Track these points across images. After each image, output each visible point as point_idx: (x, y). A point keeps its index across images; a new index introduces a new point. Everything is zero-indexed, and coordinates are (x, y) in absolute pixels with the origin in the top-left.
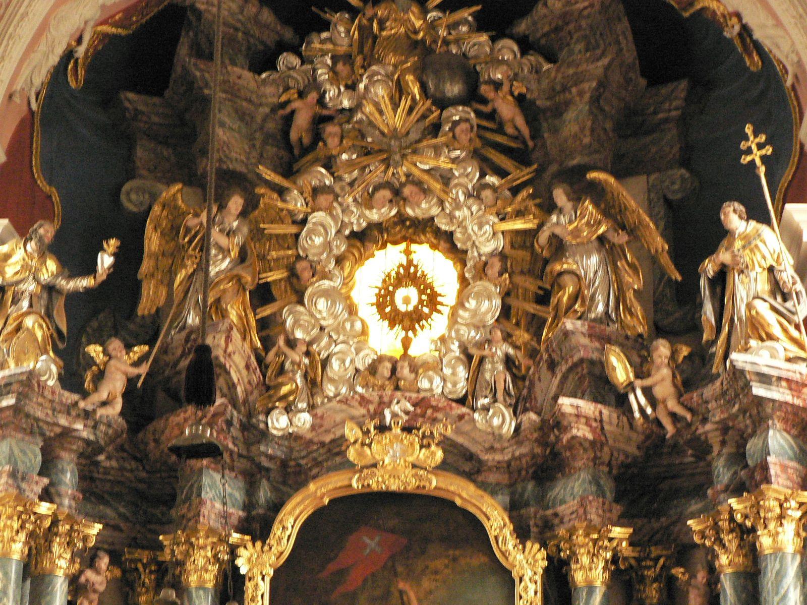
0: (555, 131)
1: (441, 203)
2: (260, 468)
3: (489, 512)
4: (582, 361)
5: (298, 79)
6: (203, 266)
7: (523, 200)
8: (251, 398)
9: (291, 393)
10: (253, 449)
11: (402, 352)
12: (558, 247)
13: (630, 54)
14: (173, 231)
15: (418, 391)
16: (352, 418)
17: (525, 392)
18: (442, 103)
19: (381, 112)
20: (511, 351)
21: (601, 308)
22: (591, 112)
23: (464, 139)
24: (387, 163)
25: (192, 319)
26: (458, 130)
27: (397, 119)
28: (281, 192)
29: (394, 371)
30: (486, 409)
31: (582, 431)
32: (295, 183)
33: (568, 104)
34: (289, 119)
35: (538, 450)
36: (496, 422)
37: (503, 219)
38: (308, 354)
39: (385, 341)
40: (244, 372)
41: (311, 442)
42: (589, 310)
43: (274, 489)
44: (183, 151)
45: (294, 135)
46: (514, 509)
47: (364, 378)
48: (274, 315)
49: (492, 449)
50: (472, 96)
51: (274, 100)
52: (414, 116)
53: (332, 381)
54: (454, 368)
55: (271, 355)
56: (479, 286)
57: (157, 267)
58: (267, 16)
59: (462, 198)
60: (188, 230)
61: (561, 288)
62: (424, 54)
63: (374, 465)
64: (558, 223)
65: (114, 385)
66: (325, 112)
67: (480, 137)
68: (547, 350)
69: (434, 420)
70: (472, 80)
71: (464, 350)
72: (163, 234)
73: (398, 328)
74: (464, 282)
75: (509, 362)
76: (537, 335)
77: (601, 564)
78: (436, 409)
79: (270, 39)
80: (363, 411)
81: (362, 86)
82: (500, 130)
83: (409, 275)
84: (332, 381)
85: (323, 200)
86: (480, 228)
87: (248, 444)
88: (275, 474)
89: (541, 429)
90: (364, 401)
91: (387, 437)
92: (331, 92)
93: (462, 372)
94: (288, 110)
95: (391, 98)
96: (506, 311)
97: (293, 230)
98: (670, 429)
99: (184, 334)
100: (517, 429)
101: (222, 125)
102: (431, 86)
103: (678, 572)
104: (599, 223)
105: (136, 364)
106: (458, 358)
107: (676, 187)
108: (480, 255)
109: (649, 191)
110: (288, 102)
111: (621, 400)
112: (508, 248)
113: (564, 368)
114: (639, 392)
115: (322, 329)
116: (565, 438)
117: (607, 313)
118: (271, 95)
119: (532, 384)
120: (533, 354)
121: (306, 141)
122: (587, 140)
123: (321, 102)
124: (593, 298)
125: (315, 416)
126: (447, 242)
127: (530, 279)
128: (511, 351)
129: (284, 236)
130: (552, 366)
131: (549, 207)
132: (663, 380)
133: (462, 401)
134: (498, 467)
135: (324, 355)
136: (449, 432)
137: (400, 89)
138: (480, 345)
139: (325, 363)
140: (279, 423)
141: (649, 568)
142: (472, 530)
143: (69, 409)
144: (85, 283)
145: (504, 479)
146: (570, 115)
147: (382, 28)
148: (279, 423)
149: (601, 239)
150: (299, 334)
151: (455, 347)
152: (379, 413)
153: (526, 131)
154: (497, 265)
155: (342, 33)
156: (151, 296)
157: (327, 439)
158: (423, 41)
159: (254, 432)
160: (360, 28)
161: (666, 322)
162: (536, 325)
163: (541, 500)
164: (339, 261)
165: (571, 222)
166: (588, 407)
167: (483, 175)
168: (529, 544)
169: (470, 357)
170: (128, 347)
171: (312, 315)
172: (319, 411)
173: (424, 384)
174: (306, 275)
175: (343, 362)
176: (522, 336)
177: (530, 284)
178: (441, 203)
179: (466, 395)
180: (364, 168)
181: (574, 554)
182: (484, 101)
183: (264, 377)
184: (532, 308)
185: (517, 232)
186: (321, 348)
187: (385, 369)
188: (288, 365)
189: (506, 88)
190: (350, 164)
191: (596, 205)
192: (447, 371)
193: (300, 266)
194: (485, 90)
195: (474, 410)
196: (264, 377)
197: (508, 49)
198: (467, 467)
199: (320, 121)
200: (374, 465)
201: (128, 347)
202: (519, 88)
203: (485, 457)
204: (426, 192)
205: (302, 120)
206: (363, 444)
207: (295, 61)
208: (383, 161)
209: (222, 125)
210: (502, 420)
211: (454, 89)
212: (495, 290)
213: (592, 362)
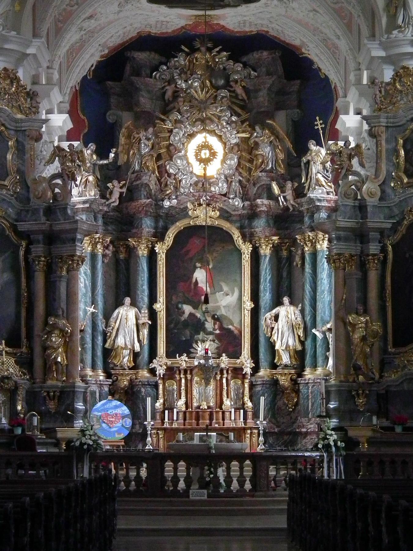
0: (256, 98)
1: (217, 126)
2: (159, 216)
3: (234, 232)
4: (264, 184)
5: (168, 77)
6: (139, 150)
7: (245, 127)
8: (157, 194)
9: (170, 193)
10: (158, 211)
11: (203, 172)
14: (129, 137)
15: (211, 192)
16: (190, 201)
17: (245, 192)
18: (217, 88)
19: (196, 92)
20: (241, 179)
21: (270, 166)
22: (268, 94)
23: (225, 104)
24: (199, 110)
25: (137, 168)
26: (223, 100)
28: (163, 121)
29: (203, 185)
30: (233, 199)
31: (264, 208)
32: (168, 117)
33: (260, 90)
34: (164, 93)
35: (250, 212)
36: (236, 203)
37: (238, 133)
38: (175, 179)
39: (198, 169)
40: (154, 186)
41: (176, 208)
42: (267, 166)
43: (164, 222)
45: (166, 97)
46: (241, 228)
47: (193, 187)
48: (162, 164)
49: (234, 210)
50: (227, 85)
51: (160, 87)
52: (208, 95)
53: (183, 187)
54: (222, 184)
55: (163, 180)
56: (230, 156)
57: (124, 149)
58: (157, 57)
59: (225, 124)
60: (134, 138)
61: (258, 160)
62: (211, 71)
63: (197, 217)
64: (256, 137)
66: (177, 89)
67: (230, 101)
68: (253, 180)
69: (216, 202)
71: (226, 177)
72: (126, 138)
73: (202, 164)
74: (225, 154)
75: (240, 182)
76: (250, 173)
77: (269, 248)
78: (217, 198)
79: (157, 63)
80: (193, 199)
81: (190, 82)
82: (236, 97)
83: (205, 146)
84: (183, 187)
85: (178, 125)
86: (231, 136)
87: (156, 209)
89: (251, 206)
90: (194, 196)
91: (201, 208)
92: (179, 82)
93: (225, 185)
94: (165, 90)
95: (200, 87)
96: (239, 164)
97: (168, 135)
98: (291, 209)
99: (136, 174)
100: (243, 205)
101: (143, 96)
102: (213, 81)
103: (293, 249)
104: (270, 137)
105: (121, 188)
106: (224, 180)
107: (296, 116)
108: (231, 144)
109: (287, 116)
110: (165, 86)
111: (276, 199)
112: (240, 142)
113: (258, 185)
114: (282, 197)
115: (179, 169)
116: (258, 210)
117: (272, 167)
118: (159, 85)
119: (248, 191)
120: (248, 181)
121: (171, 99)
122: (266, 104)
123: (176, 87)
124: (268, 162)
125: (178, 200)
126: (220, 137)
127: (247, 151)
128: (241, 179)
129: (165, 137)
130: (254, 184)
131: (254, 129)
133: (225, 195)
134: (236, 215)
135: (180, 178)
136: (221, 206)
137: (203, 86)
138: (231, 176)
139: (180, 181)
140: (167, 204)
141: (283, 246)
142: (229, 238)
143: (102, 204)
144: (105, 162)
145: (238, 218)
146: (261, 94)
147: (197, 61)
148: (167, 204)
149: (271, 142)
150: (171, 171)
151: (223, 177)
152: (199, 200)
153: (246, 98)
154: (236, 148)
155: (181, 60)
157: (182, 207)
158: (211, 65)
160: (189, 61)
161: (292, 163)
162: (250, 170)
163: (250, 226)
164: (183, 144)
165: (261, 137)
166: (266, 202)
167: (232, 115)
168: (246, 243)
169: (228, 181)
170: (119, 183)
171: (176, 165)
172: (179, 198)
173: (213, 189)
174: (174, 151)
175: (186, 181)
176: (245, 174)
177: (248, 157)
178: (217, 126)
179: (226, 193)
180: (191, 113)
181: (260, 245)
182: (232, 87)
183: (161, 186)
184: (248, 165)
185: (243, 137)
186: (180, 176)
187: (200, 185)
188: (168, 183)
189: (239, 84)
190: (187, 111)
191: (269, 130)
192: (220, 185)
193: (171, 148)
194: (231, 83)
195: (229, 198)
196: (161, 186)
197: (239, 67)
198: (226, 215)
199: (176, 94)
200: (197, 217)
201: (119, 183)
202: (243, 84)
203: (232, 213)
204: (212, 121)
205: (169, 94)
206: (194, 210)
207: (165, 68)
208: (198, 110)
209: (143, 96)
210: (238, 203)
211: (221, 82)
212: (236, 157)
213: (267, 184)
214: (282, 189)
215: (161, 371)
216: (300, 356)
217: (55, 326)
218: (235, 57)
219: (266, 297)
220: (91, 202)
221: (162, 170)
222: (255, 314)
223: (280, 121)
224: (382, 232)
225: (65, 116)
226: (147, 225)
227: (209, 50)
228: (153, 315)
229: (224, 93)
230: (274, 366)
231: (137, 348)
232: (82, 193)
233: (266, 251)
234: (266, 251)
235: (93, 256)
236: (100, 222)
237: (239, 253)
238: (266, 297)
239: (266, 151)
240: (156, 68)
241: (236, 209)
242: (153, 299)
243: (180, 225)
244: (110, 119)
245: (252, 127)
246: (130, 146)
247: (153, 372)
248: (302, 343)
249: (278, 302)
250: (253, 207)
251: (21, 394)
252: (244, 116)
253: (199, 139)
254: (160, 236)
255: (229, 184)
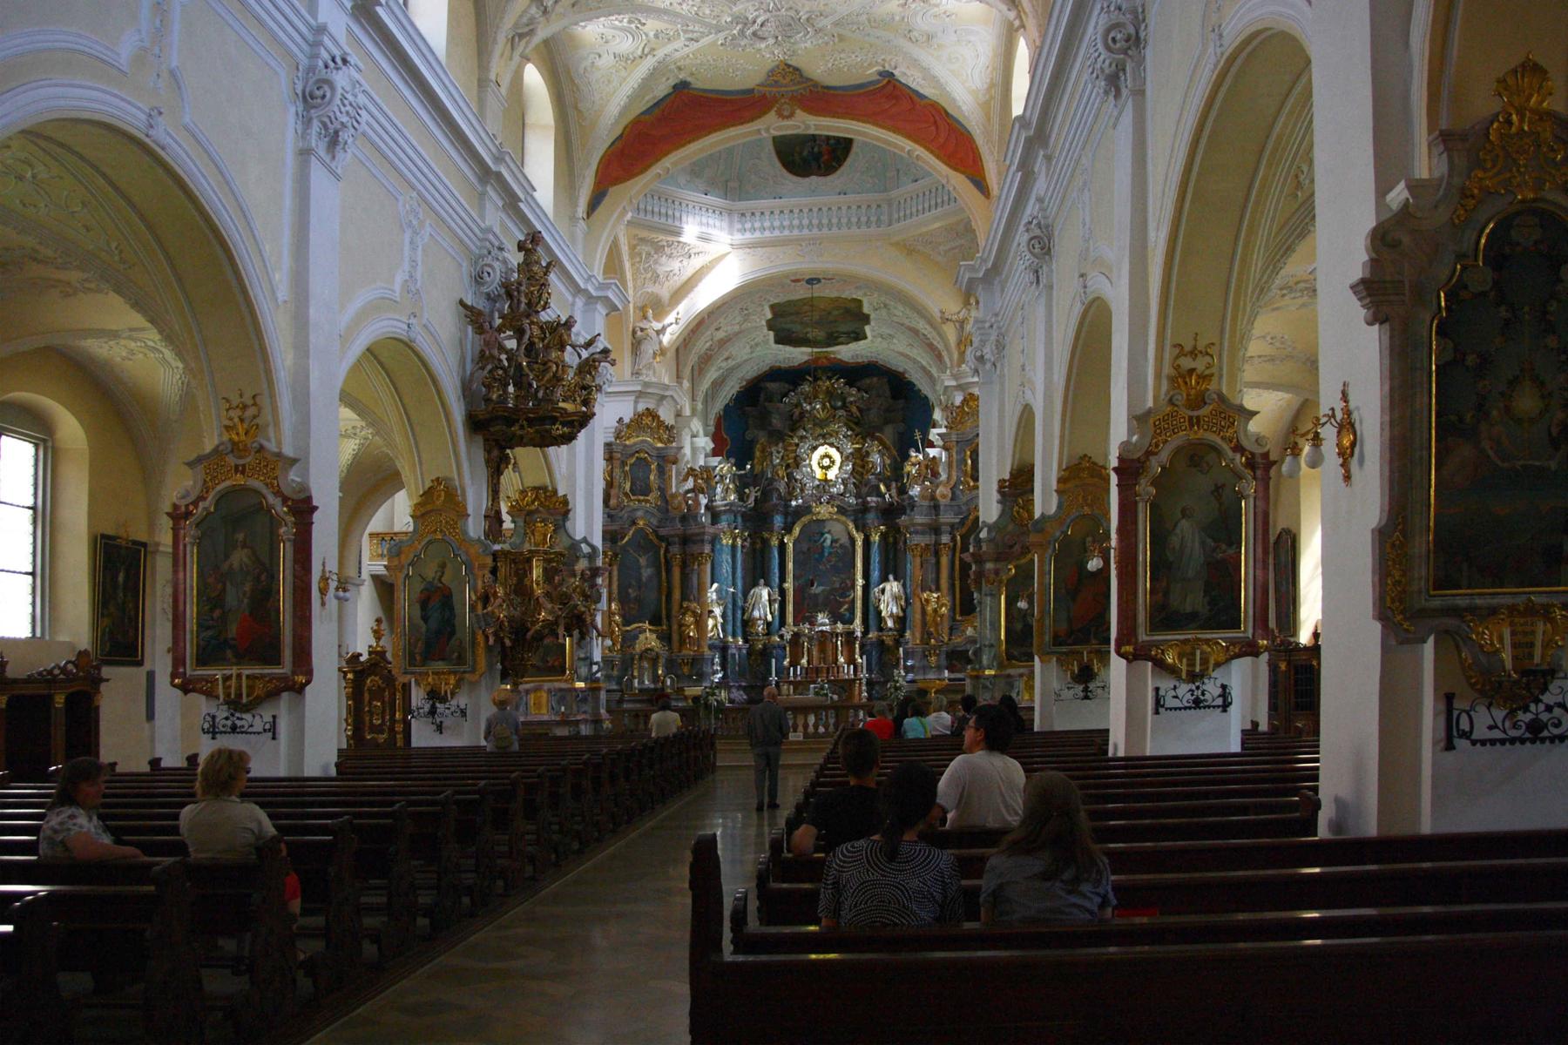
12: (868, 454)
13: (888, 393)
14: (763, 451)
18: (835, 408)
27: (822, 415)
44: (763, 421)
50: (844, 407)
62: (830, 394)
65: (752, 500)
70: (844, 400)
83: (827, 456)
88: (793, 516)
111: (882, 496)
127: (859, 460)
132: (894, 492)
155: (806, 388)
156: (758, 469)
159: (787, 506)
210: (852, 500)
214: (888, 488)
215: (788, 637)
216: (901, 621)
217: (688, 609)
218: (850, 384)
219: (875, 574)
220: (731, 504)
221: (790, 476)
222: (866, 589)
223: (888, 434)
224: (952, 526)
225: (708, 439)
226: (778, 520)
227: (830, 378)
228: (782, 592)
229: (841, 412)
230: (881, 629)
231: (769, 618)
232: (724, 495)
233: (876, 538)
234: (876, 538)
235: (734, 547)
236: (739, 519)
237: (853, 541)
238: (875, 574)
239: (876, 458)
240: (786, 395)
241: (850, 505)
242: (783, 579)
243: (805, 519)
244: (749, 436)
245: (864, 439)
246: (764, 458)
247: (781, 637)
248: (904, 610)
249: (885, 579)
250: (865, 503)
251: (662, 661)
252: (858, 430)
253: (822, 450)
254: (788, 529)
255: (845, 485)
